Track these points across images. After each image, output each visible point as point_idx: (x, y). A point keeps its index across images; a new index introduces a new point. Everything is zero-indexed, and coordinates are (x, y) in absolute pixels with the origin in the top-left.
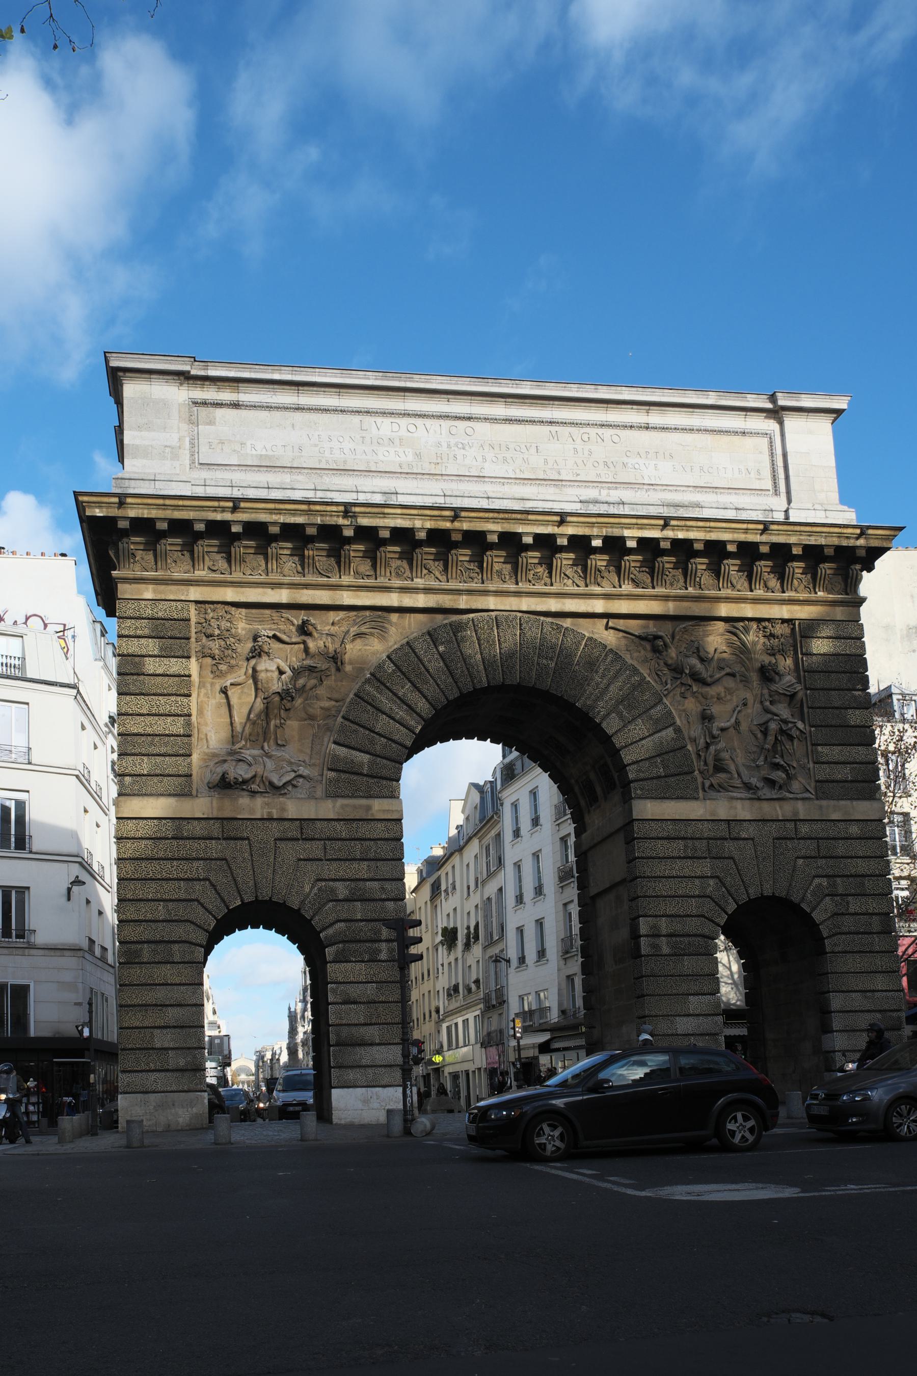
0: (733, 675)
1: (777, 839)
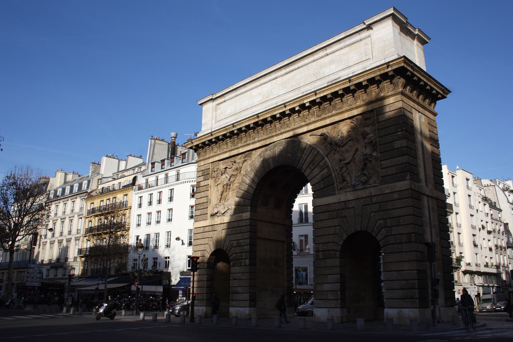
1: (364, 205)
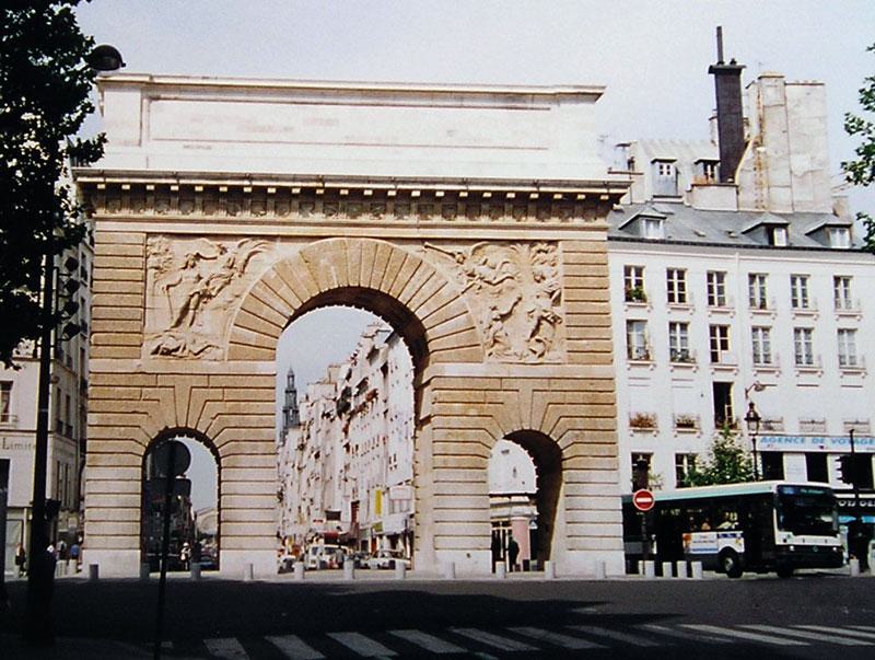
0: (512, 278)
